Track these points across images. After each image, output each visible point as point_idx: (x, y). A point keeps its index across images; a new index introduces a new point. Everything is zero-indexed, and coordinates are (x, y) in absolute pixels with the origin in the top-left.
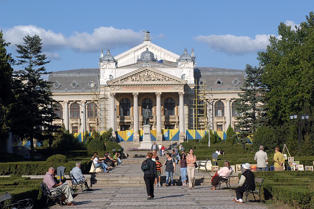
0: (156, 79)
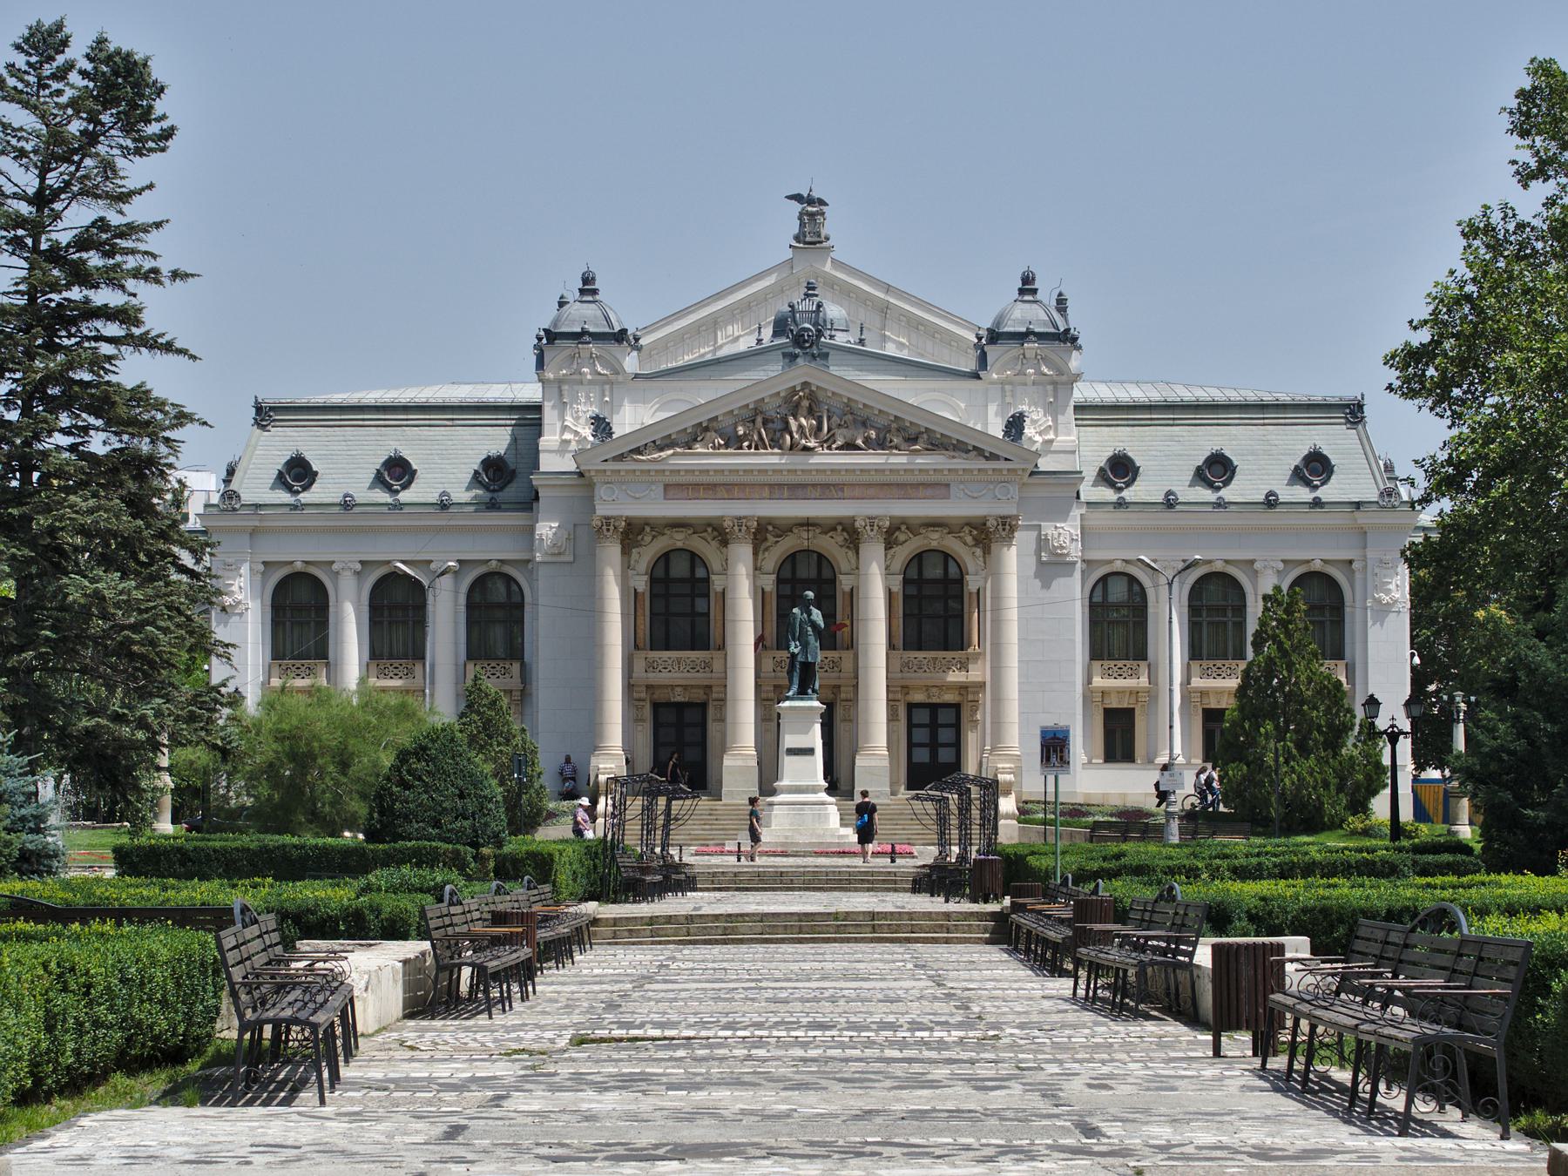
0: (859, 442)
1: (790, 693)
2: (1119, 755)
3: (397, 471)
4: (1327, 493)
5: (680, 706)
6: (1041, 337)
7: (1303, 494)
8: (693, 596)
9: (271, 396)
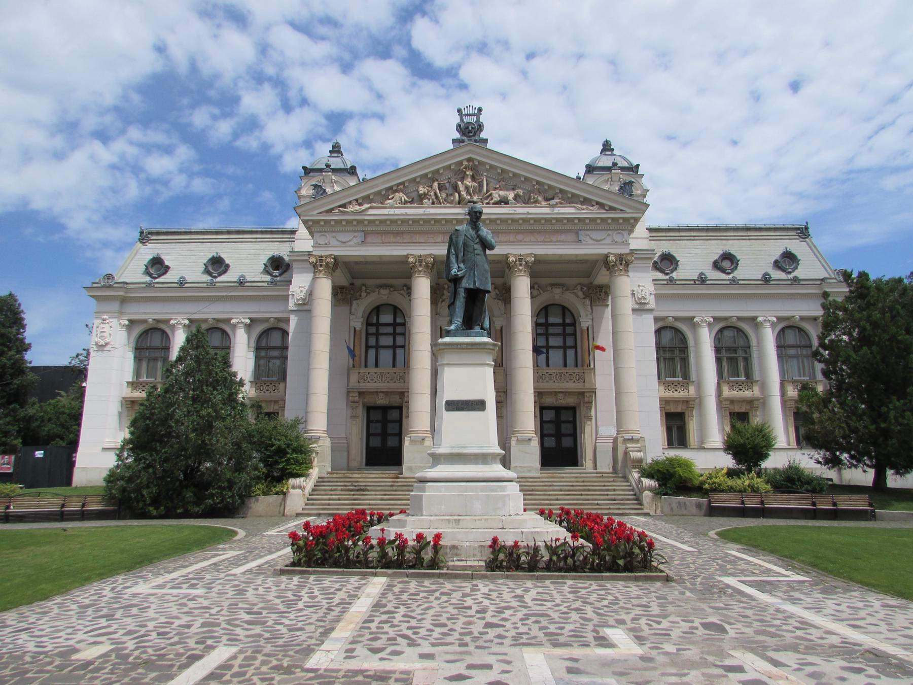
1: (452, 327)
3: (217, 265)
4: (800, 273)
5: (385, 409)
6: (623, 169)
7: (780, 275)
8: (394, 334)
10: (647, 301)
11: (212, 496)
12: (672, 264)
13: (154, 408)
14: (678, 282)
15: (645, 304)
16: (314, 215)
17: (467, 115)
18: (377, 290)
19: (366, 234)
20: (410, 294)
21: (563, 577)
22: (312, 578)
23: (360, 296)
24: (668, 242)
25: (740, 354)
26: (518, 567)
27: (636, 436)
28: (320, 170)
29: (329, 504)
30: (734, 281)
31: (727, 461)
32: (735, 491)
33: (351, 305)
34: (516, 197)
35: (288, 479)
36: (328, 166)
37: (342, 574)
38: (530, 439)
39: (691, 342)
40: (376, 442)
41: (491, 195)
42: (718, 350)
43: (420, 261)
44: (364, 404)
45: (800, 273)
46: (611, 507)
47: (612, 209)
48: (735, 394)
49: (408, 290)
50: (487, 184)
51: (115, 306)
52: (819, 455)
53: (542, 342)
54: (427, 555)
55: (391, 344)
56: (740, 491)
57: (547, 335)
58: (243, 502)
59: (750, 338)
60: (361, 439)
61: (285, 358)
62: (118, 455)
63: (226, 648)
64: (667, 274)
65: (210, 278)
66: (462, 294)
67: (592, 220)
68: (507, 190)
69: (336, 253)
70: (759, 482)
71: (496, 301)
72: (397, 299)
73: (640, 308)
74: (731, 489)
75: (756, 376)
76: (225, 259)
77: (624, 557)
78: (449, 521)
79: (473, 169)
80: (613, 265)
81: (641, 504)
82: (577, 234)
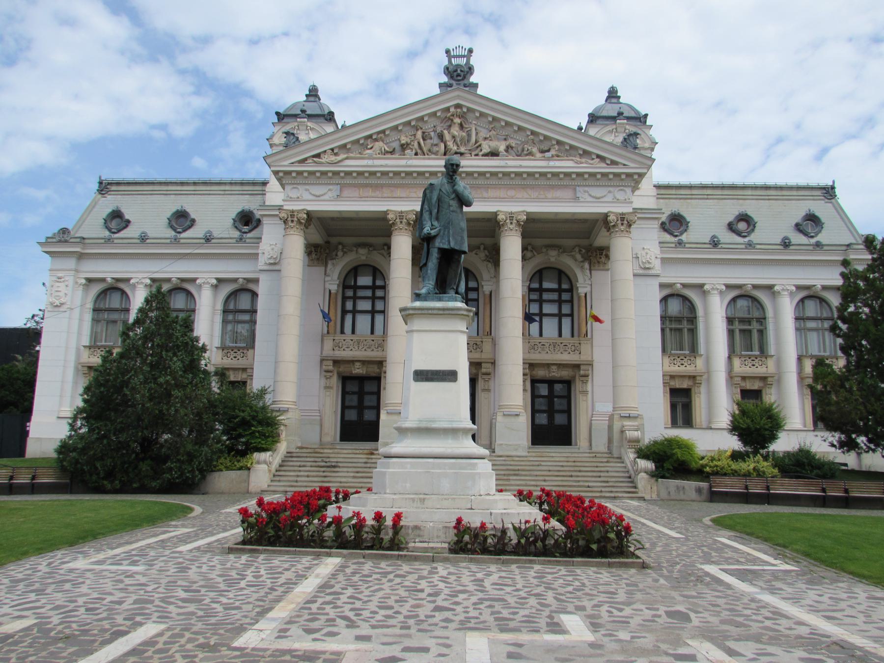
0: (502, 148)
2: (680, 421)
4: (822, 238)
5: (361, 380)
6: (628, 118)
7: (803, 239)
8: (373, 298)
9: (109, 175)
10: (651, 266)
11: (170, 470)
12: (681, 225)
13: (109, 374)
14: (687, 246)
15: (649, 268)
16: (285, 165)
17: (455, 57)
18: (355, 249)
19: (343, 187)
20: (389, 254)
21: (531, 562)
22: (262, 556)
23: (336, 255)
24: (678, 201)
25: (755, 326)
26: (485, 551)
27: (633, 413)
28: (295, 116)
29: (297, 481)
30: (750, 245)
31: (734, 443)
32: (739, 475)
33: (326, 266)
34: (508, 148)
35: (252, 453)
36: (303, 111)
37: (295, 553)
38: (517, 415)
39: (700, 312)
40: (352, 415)
41: (480, 145)
42: (730, 320)
43: (401, 217)
44: (339, 374)
45: (822, 238)
46: (603, 489)
47: (614, 163)
48: (748, 370)
49: (387, 248)
50: (477, 133)
51: (71, 263)
52: (835, 437)
53: (534, 309)
54: (387, 535)
55: (370, 309)
56: (745, 475)
57: (541, 302)
58: (204, 478)
59: (694, 303)
60: (335, 412)
61: (253, 322)
62: (70, 425)
63: (154, 625)
64: (676, 236)
65: (173, 233)
66: (435, 255)
67: (592, 175)
68: (498, 140)
69: (310, 208)
70: (765, 466)
71: (485, 263)
72: (376, 259)
73: (644, 273)
74: (735, 473)
75: (772, 350)
76: (191, 214)
77: (598, 542)
78: (413, 500)
79: (462, 116)
80: (614, 226)
81: (635, 487)
82: (575, 190)
